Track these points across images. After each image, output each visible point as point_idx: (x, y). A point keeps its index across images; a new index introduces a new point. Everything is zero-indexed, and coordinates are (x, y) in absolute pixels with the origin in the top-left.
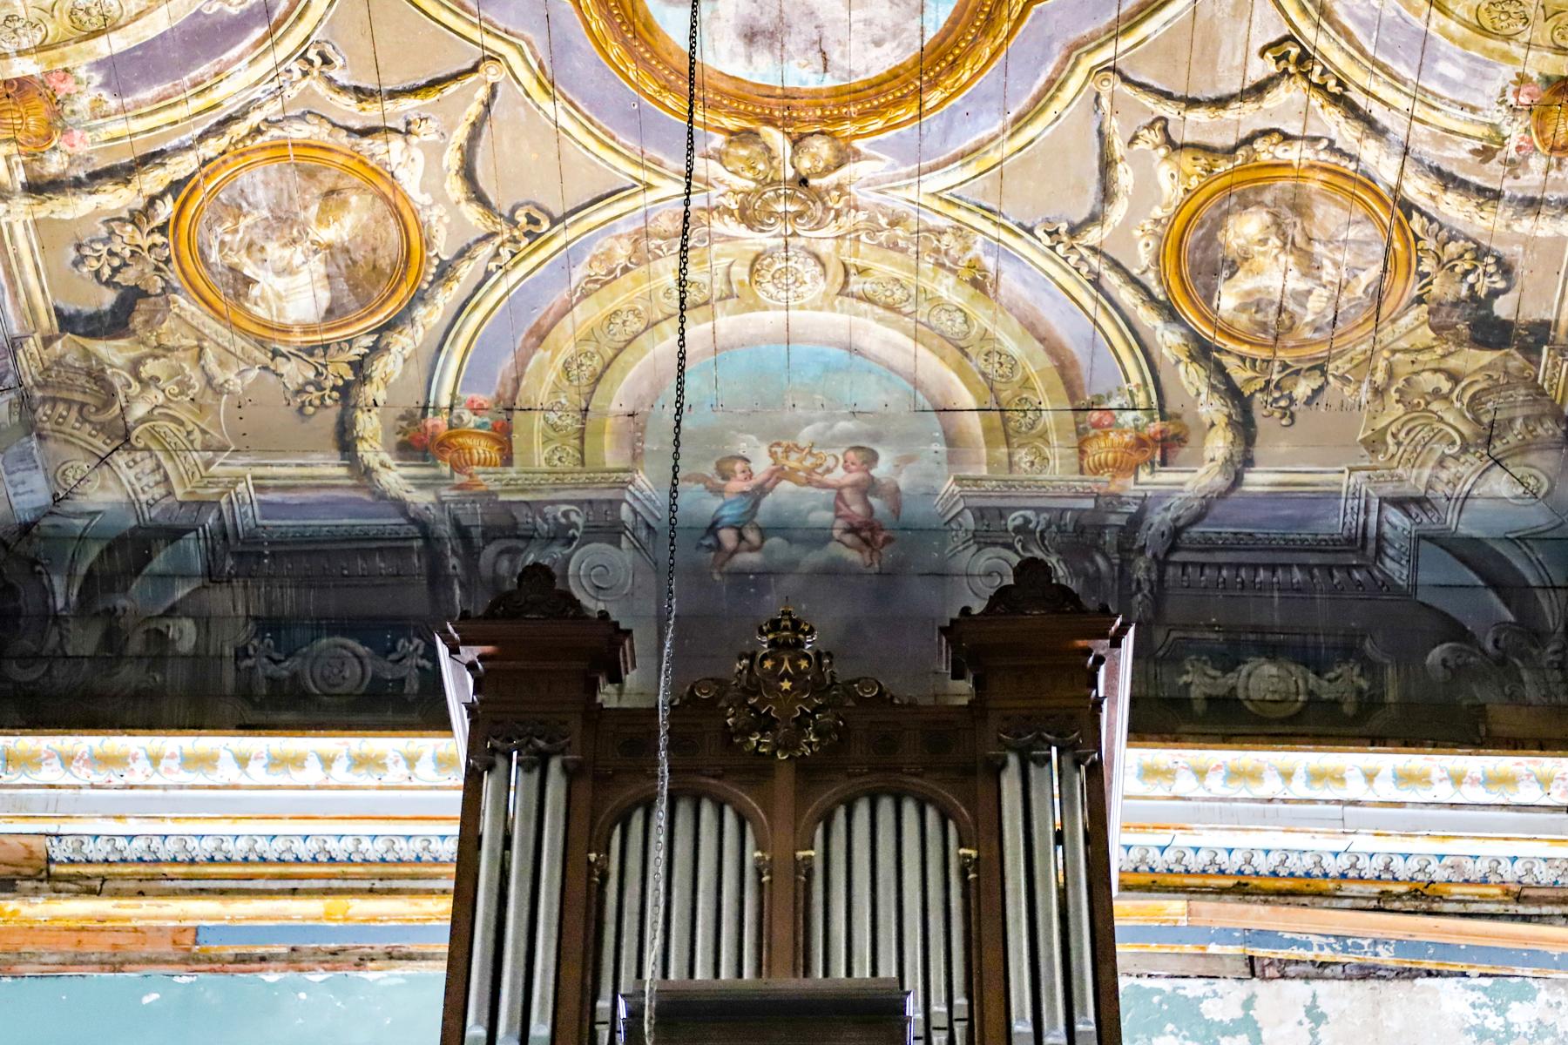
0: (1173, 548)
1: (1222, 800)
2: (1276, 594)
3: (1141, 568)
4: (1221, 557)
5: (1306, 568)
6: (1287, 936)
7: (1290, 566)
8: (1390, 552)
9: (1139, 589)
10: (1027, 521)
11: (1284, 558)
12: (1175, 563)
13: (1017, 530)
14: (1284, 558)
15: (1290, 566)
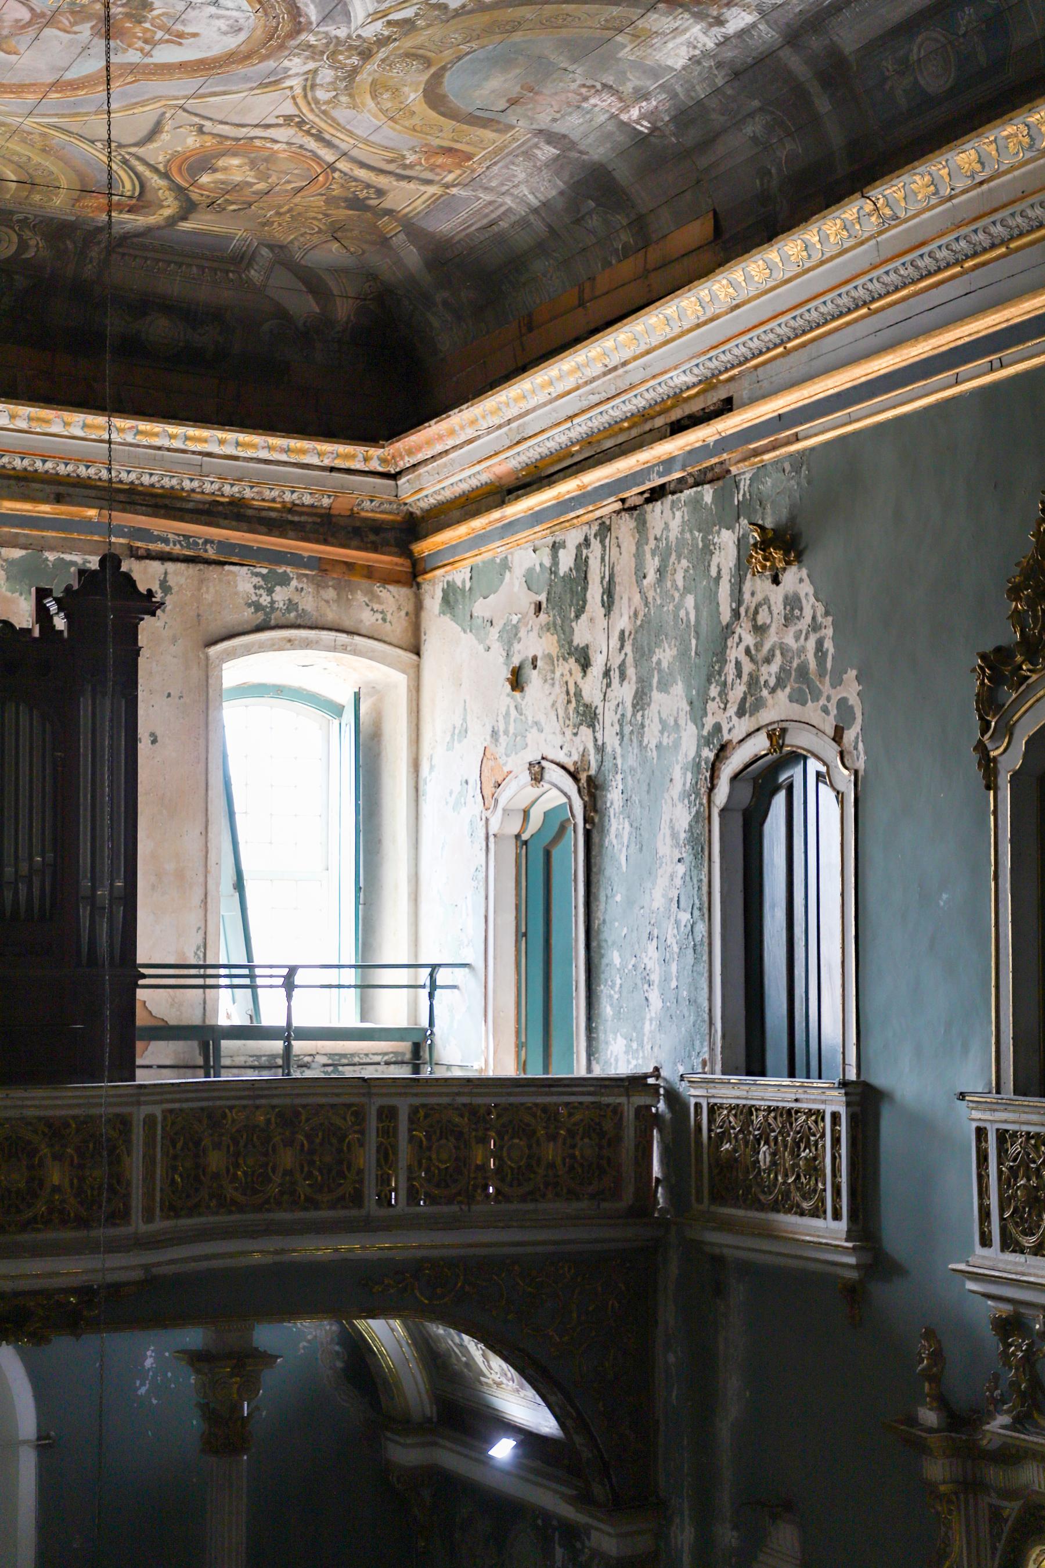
0: (119, 245)
1: (131, 445)
2: (178, 278)
3: (94, 253)
4: (149, 254)
5: (202, 268)
6: (155, 533)
7: (191, 265)
8: (256, 267)
9: (91, 261)
10: (26, 218)
11: (189, 260)
12: (119, 253)
13: (18, 221)
14: (189, 260)
15: (191, 265)
